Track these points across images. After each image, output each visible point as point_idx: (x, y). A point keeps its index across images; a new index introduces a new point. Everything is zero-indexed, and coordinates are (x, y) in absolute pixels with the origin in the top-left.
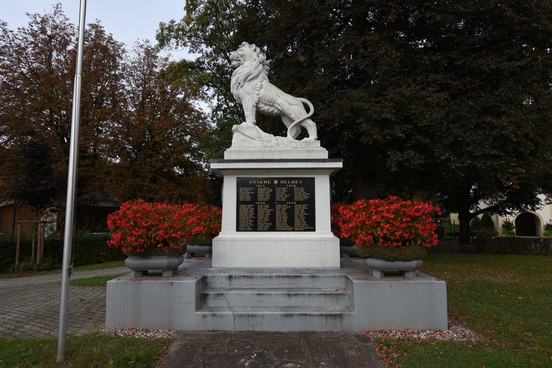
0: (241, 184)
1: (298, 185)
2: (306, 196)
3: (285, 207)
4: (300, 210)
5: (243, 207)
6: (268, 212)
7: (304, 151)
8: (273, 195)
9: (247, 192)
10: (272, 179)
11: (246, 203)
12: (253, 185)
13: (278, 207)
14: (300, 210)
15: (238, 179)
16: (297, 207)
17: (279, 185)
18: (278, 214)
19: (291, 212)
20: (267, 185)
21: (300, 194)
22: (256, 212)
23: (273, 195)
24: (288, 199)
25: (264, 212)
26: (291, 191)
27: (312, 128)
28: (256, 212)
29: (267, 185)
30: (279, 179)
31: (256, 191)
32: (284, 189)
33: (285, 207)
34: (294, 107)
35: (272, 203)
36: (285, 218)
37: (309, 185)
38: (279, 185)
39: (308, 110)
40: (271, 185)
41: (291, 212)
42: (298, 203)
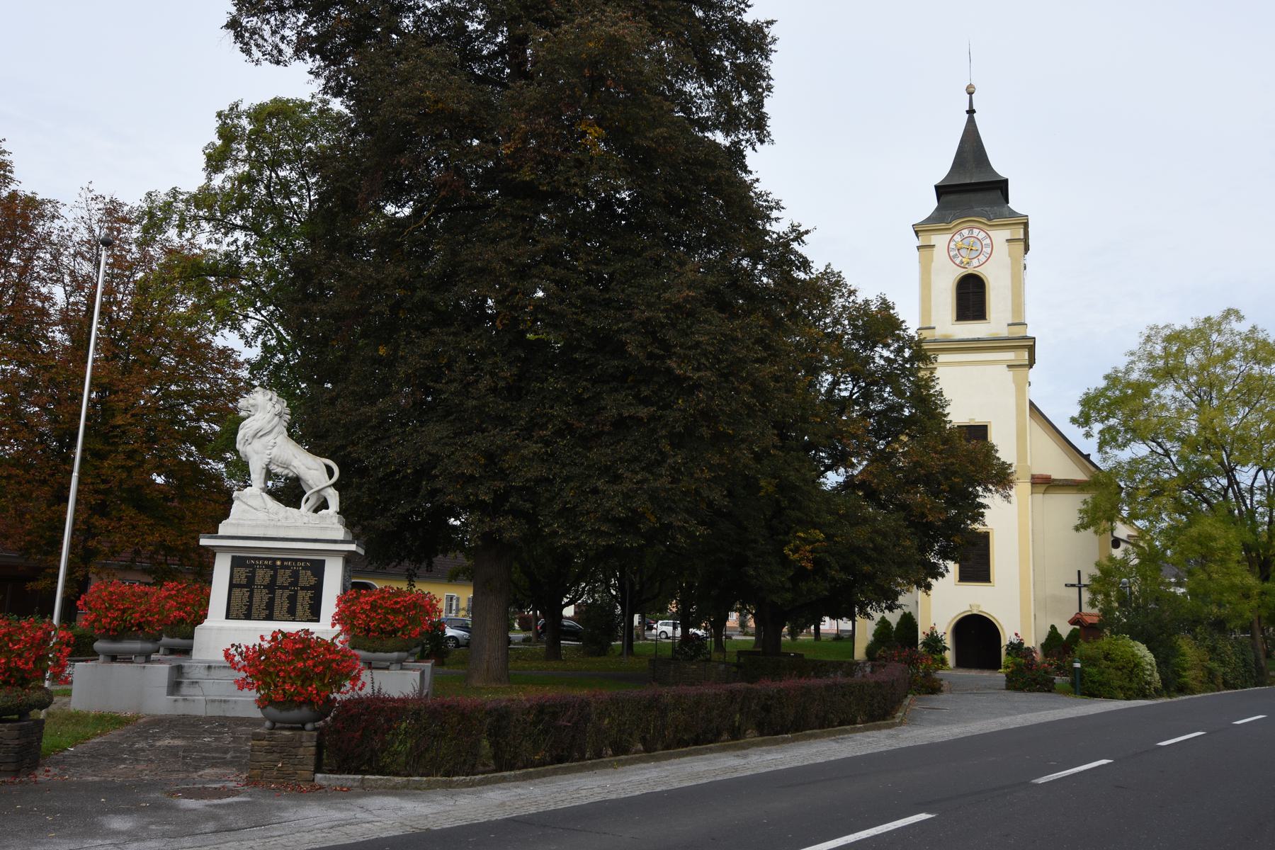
0: (237, 563)
1: (305, 568)
2: (313, 581)
3: (287, 593)
4: (304, 597)
5: (236, 591)
6: (266, 599)
8: (274, 578)
9: (242, 573)
10: (275, 560)
11: (240, 586)
12: (251, 566)
13: (279, 592)
14: (304, 597)
15: (233, 557)
16: (301, 594)
17: (282, 567)
18: (277, 601)
19: (293, 600)
20: (267, 567)
21: (306, 578)
22: (251, 597)
23: (274, 578)
24: (291, 584)
25: (261, 597)
26: (295, 575)
27: (333, 498)
28: (251, 597)
29: (267, 567)
30: (283, 560)
31: (253, 573)
32: (288, 572)
33: (287, 593)
34: (314, 471)
35: (271, 587)
36: (286, 605)
37: (317, 568)
38: (282, 567)
39: (330, 472)
40: (273, 567)
41: (293, 600)
42: (303, 588)
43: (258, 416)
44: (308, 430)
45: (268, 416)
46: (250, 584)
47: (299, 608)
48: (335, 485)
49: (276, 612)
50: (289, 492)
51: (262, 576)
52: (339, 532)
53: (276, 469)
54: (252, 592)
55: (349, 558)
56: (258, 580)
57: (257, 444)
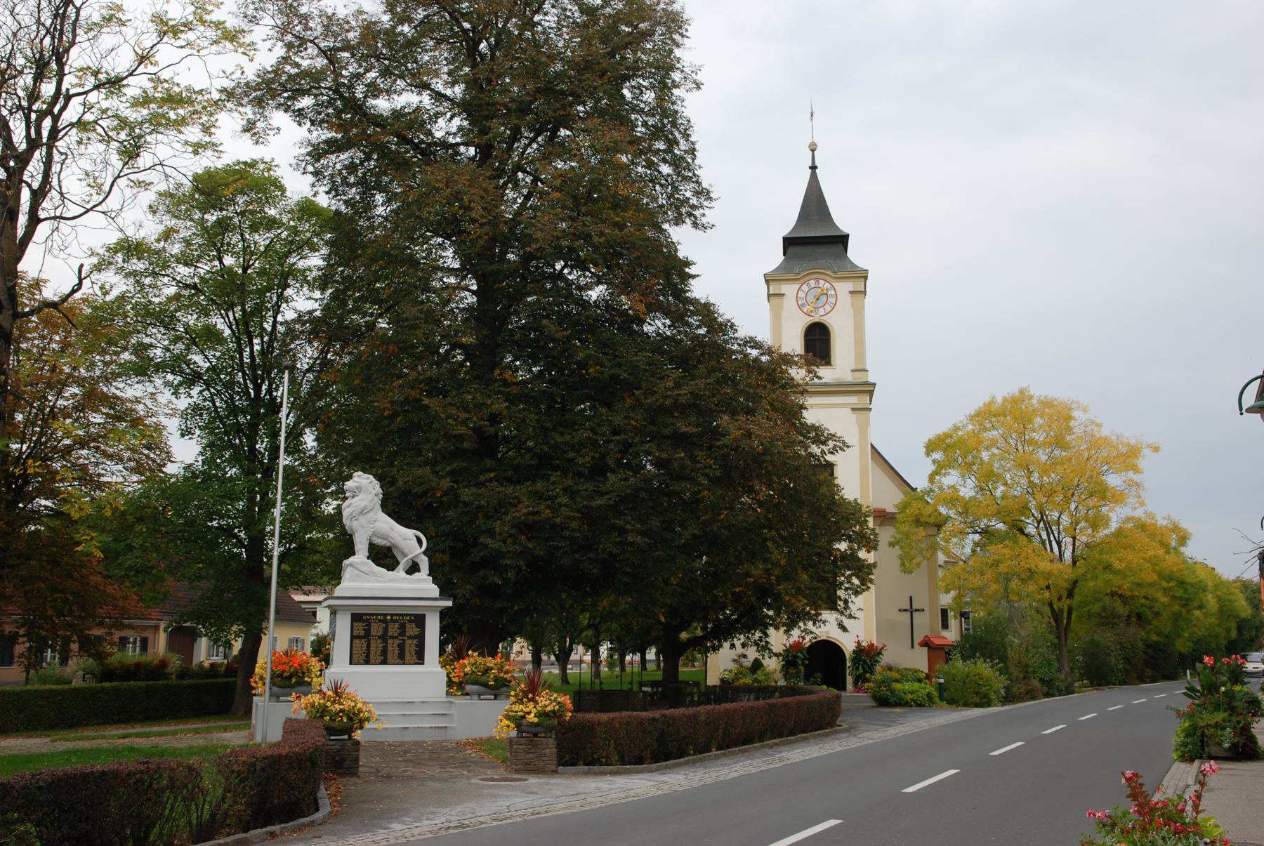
0: (356, 618)
1: (410, 621)
2: (417, 631)
3: (397, 642)
4: (411, 645)
5: (356, 641)
6: (380, 648)
7: (416, 588)
8: (386, 630)
9: (360, 627)
10: (385, 615)
11: (359, 637)
12: (367, 620)
13: (390, 641)
14: (411, 645)
15: (353, 615)
16: (408, 642)
17: (392, 620)
18: (390, 648)
19: (402, 647)
20: (380, 621)
21: (412, 630)
22: (368, 646)
23: (386, 630)
24: (400, 634)
25: (376, 646)
26: (402, 627)
27: (424, 563)
28: (368, 646)
29: (380, 621)
30: (392, 615)
31: (369, 625)
32: (397, 625)
33: (397, 642)
34: (408, 540)
35: (384, 637)
36: (397, 651)
37: (420, 620)
38: (392, 620)
39: (420, 541)
40: (384, 621)
41: (402, 647)
42: (409, 638)
43: (361, 496)
44: (398, 506)
45: (371, 497)
46: (367, 634)
47: (407, 654)
48: (424, 553)
49: (408, 657)
50: (384, 556)
51: (377, 629)
52: (434, 590)
53: (378, 541)
54: (369, 642)
55: (444, 614)
56: (373, 632)
57: (362, 520)
